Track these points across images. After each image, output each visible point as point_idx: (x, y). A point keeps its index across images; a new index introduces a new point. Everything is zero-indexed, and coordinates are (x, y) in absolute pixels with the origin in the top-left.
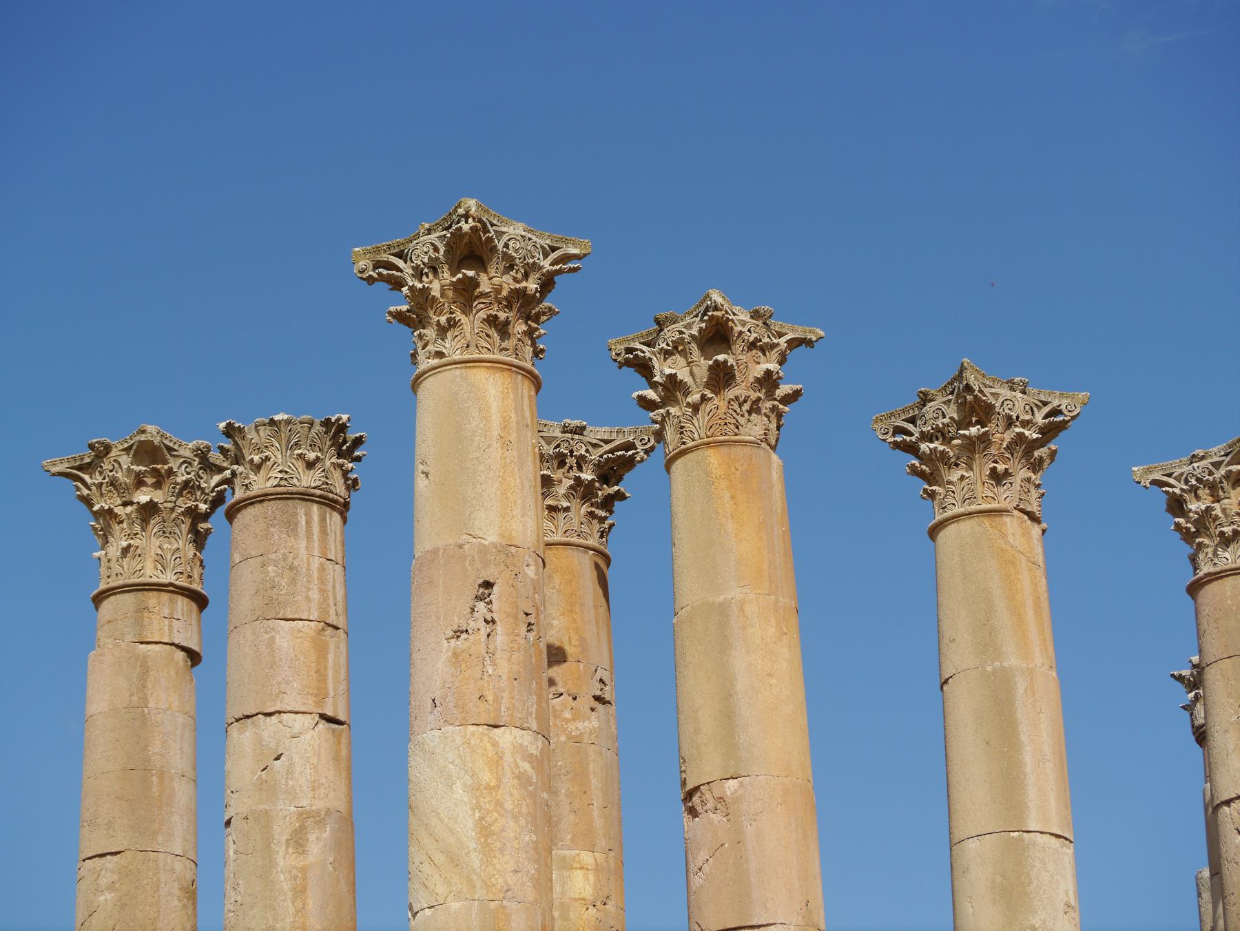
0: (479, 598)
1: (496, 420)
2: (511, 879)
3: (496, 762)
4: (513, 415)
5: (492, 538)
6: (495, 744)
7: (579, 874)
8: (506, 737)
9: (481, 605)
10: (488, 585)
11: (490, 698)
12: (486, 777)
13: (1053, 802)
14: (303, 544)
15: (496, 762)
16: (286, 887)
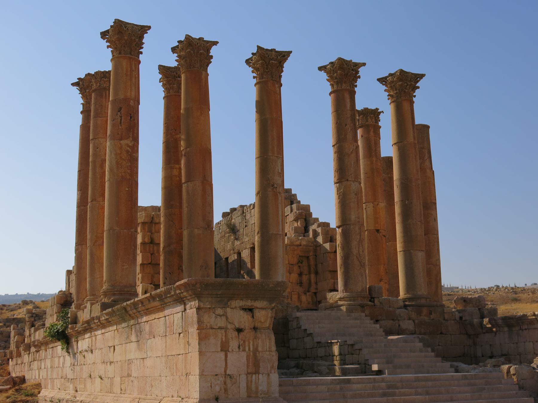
0: (119, 111)
1: (125, 69)
2: (123, 174)
3: (121, 148)
4: (129, 69)
5: (122, 97)
6: (121, 144)
7: (175, 170)
8: (123, 142)
9: (119, 113)
10: (121, 108)
11: (120, 133)
12: (118, 152)
13: (276, 149)
14: (104, 100)
15: (121, 148)
16: (99, 177)
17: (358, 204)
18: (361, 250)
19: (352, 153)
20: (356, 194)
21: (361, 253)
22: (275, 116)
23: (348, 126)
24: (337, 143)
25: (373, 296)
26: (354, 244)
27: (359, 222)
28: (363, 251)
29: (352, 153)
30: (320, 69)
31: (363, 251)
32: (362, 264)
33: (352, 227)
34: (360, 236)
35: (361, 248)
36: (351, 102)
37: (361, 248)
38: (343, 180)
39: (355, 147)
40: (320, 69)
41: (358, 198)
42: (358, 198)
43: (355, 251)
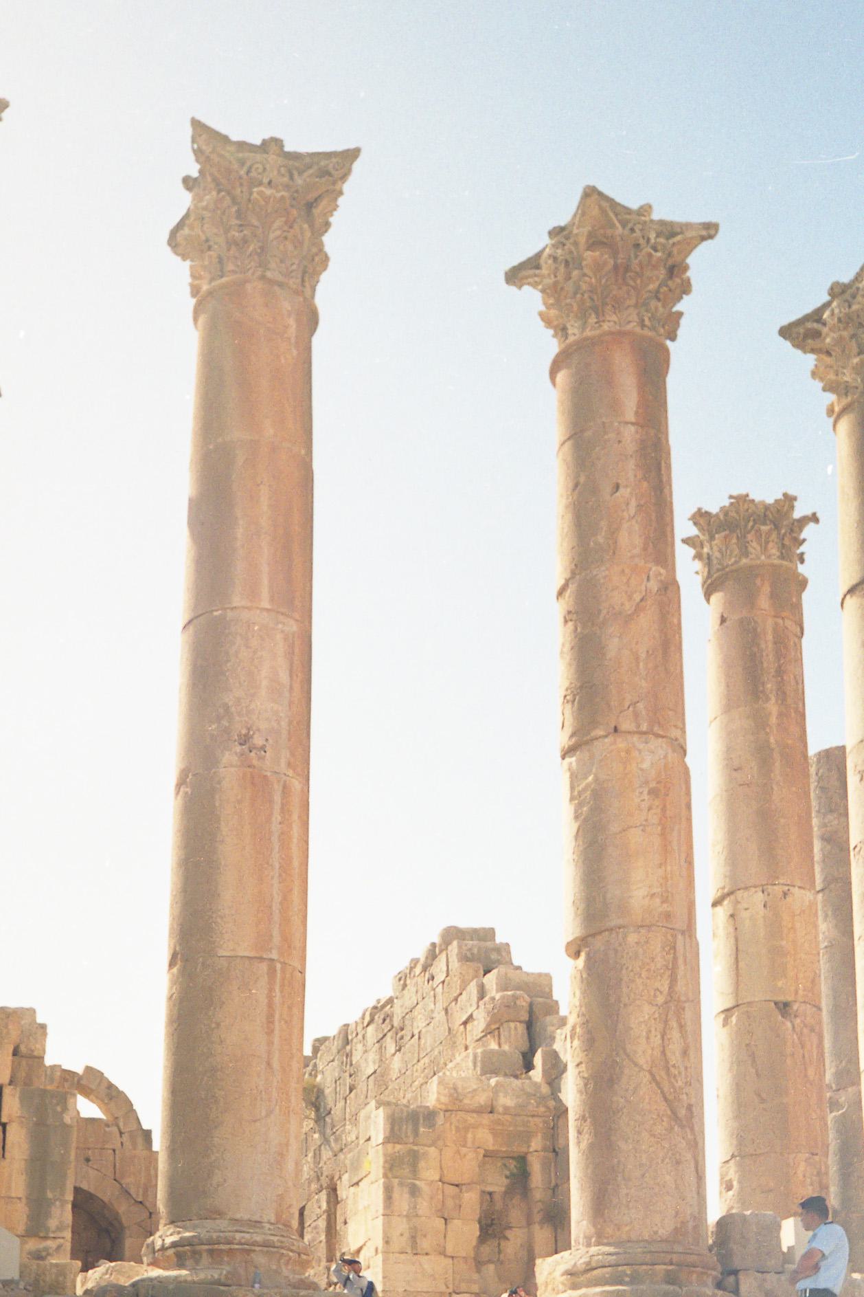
17: (663, 835)
18: (675, 1048)
19: (638, 609)
20: (653, 792)
21: (675, 1058)
22: (269, 431)
23: (624, 492)
24: (573, 573)
25: (737, 1263)
26: (641, 1018)
27: (668, 916)
28: (685, 1053)
29: (638, 609)
30: (515, 276)
31: (685, 1053)
32: (682, 1112)
33: (632, 938)
34: (673, 980)
35: (675, 1034)
36: (641, 388)
37: (675, 1034)
38: (600, 732)
39: (654, 585)
40: (515, 276)
41: (664, 810)
42: (664, 810)
43: (643, 1050)
